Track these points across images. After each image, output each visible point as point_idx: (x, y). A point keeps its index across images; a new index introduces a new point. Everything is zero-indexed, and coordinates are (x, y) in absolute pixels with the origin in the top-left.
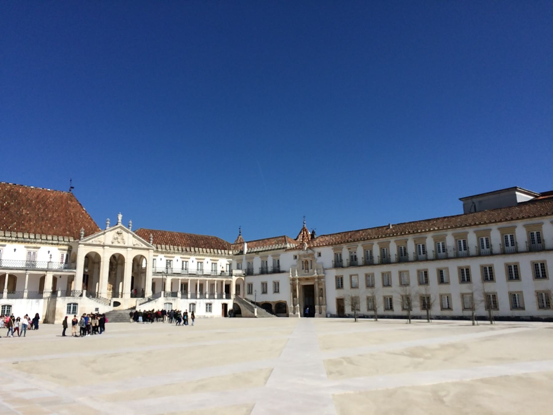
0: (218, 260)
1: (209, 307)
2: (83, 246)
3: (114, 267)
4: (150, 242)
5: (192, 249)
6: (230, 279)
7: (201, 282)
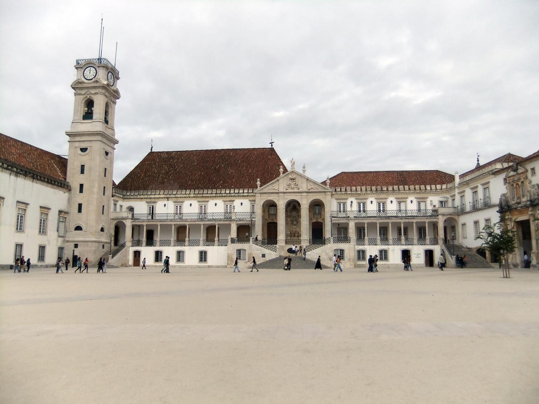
0: (427, 198)
2: (259, 195)
4: (326, 185)
5: (390, 188)
6: (435, 220)
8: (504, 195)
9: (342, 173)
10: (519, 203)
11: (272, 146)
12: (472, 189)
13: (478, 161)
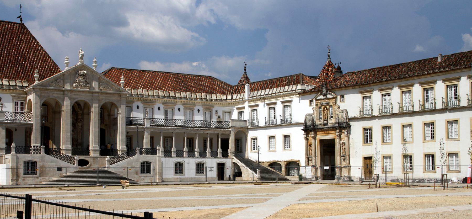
1: (200, 168)
3: (80, 117)
7: (190, 136)
8: (310, 115)
9: (112, 68)
10: (327, 124)
11: (21, 20)
12: (268, 104)
13: (245, 70)
